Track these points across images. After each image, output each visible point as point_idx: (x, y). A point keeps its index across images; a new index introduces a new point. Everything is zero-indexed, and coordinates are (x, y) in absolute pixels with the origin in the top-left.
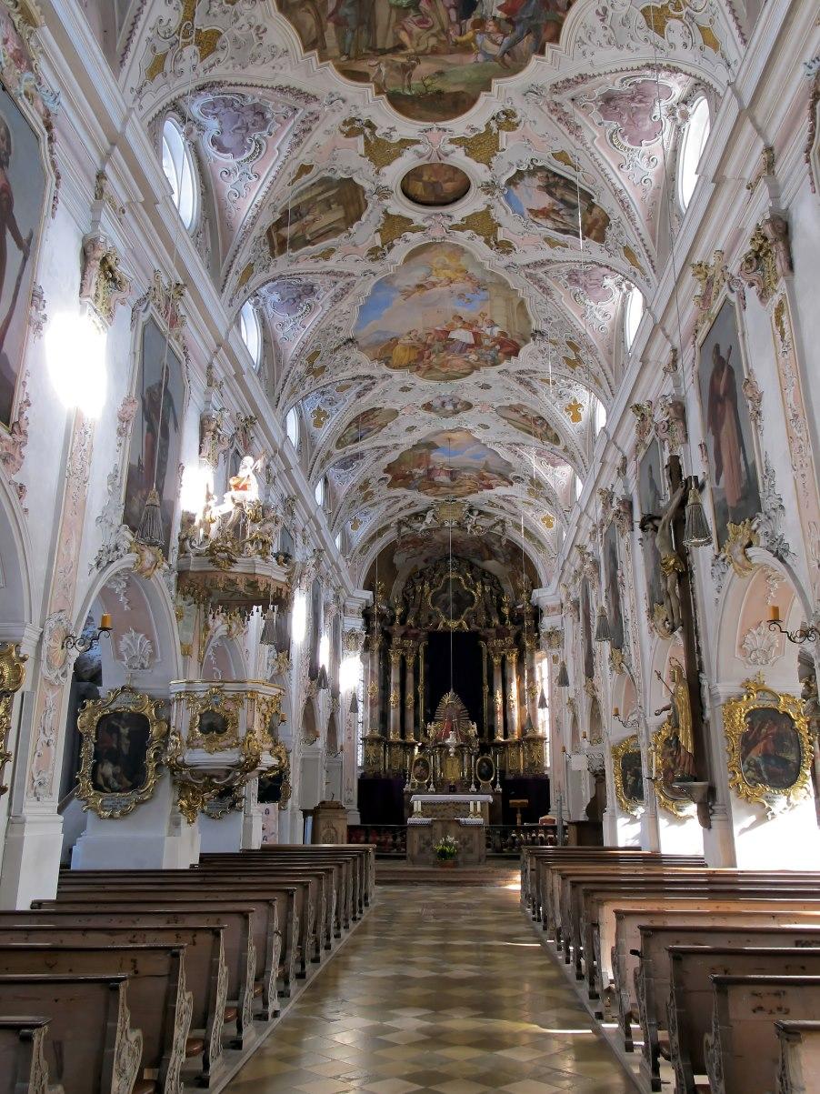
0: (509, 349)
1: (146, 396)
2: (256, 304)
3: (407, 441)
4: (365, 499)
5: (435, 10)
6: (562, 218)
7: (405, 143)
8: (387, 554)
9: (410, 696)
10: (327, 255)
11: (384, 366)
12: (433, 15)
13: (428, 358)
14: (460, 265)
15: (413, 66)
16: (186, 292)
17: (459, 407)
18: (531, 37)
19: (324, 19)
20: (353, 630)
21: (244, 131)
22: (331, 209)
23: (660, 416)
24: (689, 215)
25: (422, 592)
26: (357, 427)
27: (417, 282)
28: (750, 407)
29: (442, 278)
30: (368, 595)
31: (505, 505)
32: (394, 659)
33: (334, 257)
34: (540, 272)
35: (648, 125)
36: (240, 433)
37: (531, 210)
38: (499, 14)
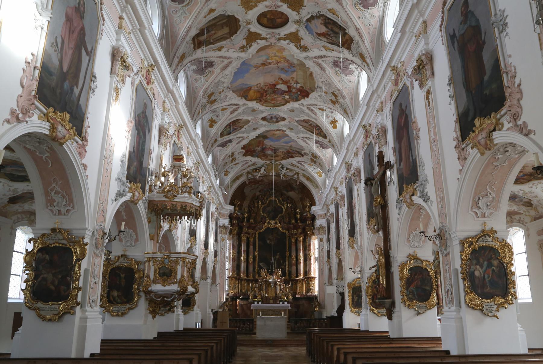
0: (304, 94)
1: (137, 119)
2: (184, 70)
3: (254, 135)
4: (232, 161)
8: (242, 187)
9: (251, 257)
10: (220, 49)
11: (244, 99)
13: (265, 97)
16: (155, 68)
17: (279, 119)
20: (224, 225)
23: (374, 132)
24: (389, 46)
25: (258, 206)
26: (230, 128)
27: (262, 62)
28: (415, 134)
29: (274, 61)
30: (232, 208)
31: (299, 165)
32: (244, 238)
33: (224, 50)
34: (320, 61)
36: (176, 133)
37: (317, 33)
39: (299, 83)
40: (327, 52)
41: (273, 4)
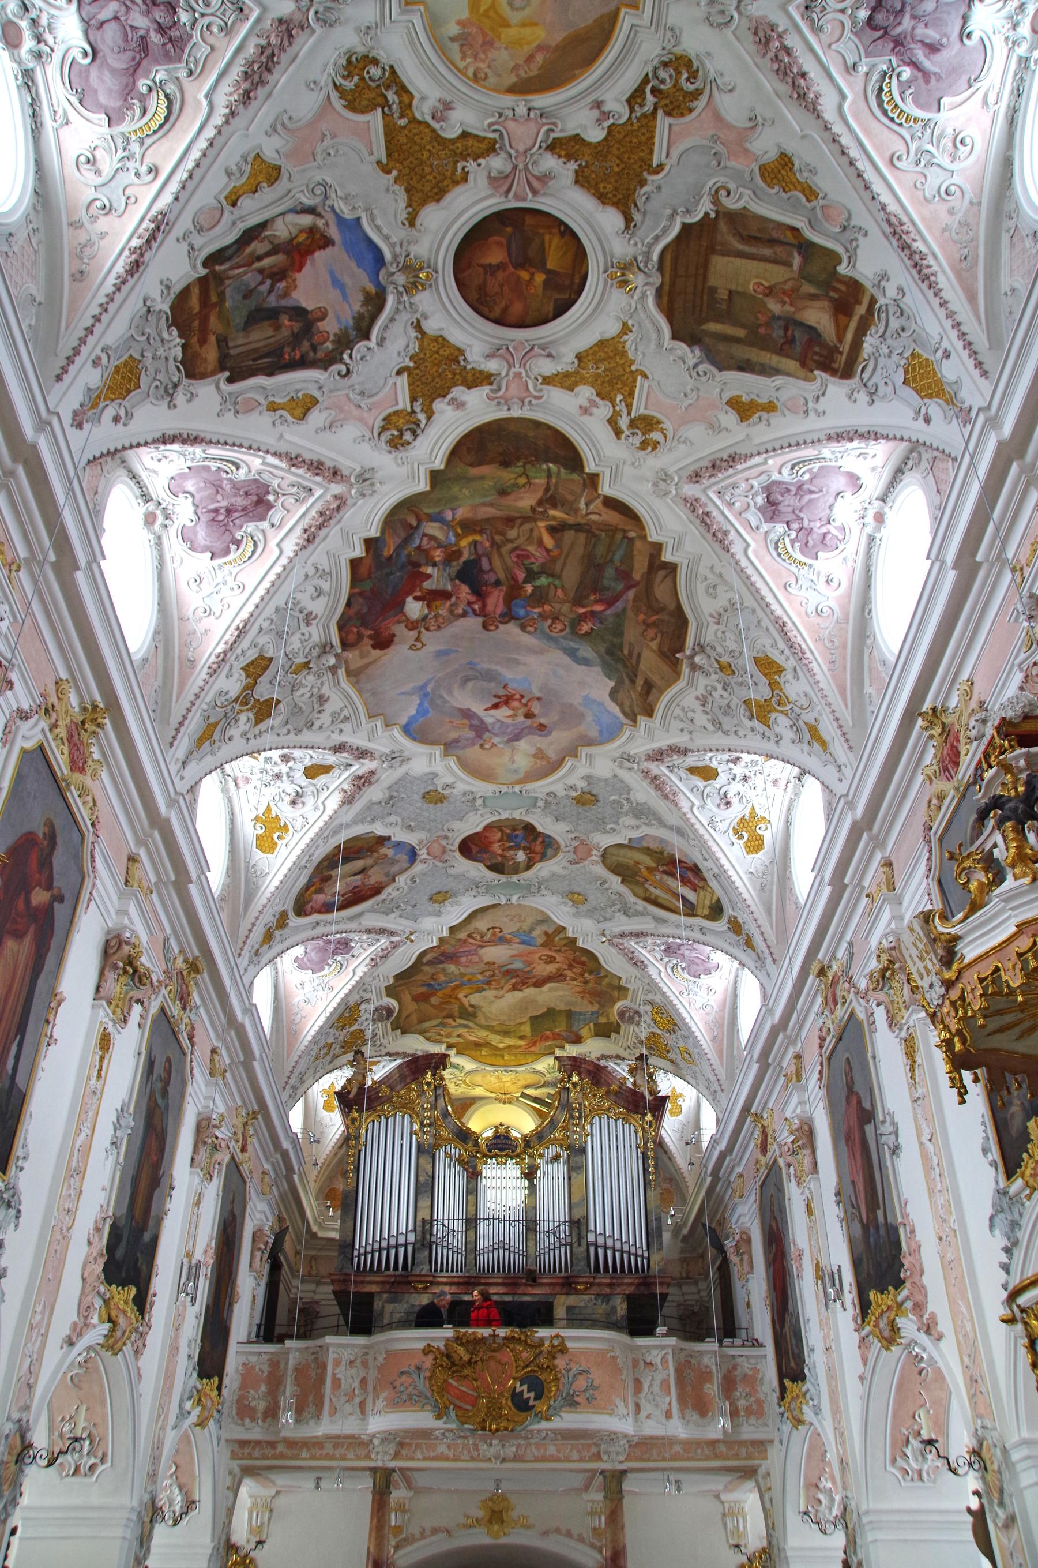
5: (506, 568)
6: (261, 271)
7: (566, 381)
12: (510, 564)
15: (540, 503)
16: (927, 706)
18: (386, 553)
21: (806, 487)
37: (327, 242)
38: (429, 570)
41: (517, 369)
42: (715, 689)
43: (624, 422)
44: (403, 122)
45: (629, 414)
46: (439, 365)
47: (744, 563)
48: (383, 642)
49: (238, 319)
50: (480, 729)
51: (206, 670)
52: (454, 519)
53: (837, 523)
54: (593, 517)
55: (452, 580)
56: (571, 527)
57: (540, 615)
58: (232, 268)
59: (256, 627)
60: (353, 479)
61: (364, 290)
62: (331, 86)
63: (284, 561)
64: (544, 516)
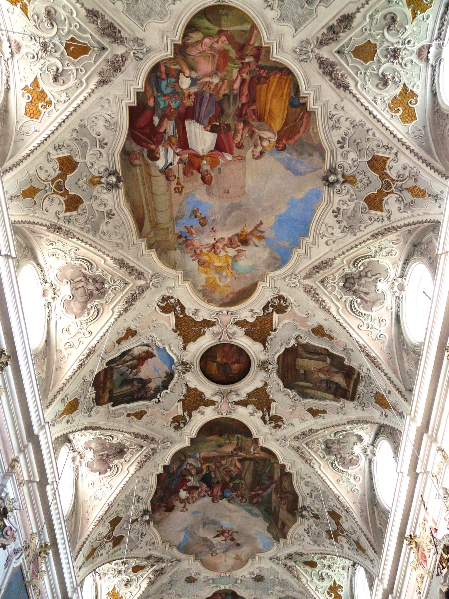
6: (127, 366)
7: (244, 403)
12: (223, 475)
13: (243, 81)
14: (206, 273)
15: (235, 450)
19: (278, 482)
22: (305, 371)
35: (93, 445)
37: (152, 356)
38: (190, 478)
39: (162, 171)
40: (126, 326)
42: (312, 526)
43: (267, 418)
44: (182, 316)
45: (269, 415)
46: (194, 398)
47: (319, 472)
48: (170, 509)
49: (117, 383)
50: (211, 546)
51: (93, 524)
52: (200, 457)
53: (356, 455)
54: (256, 455)
55: (199, 482)
56: (248, 459)
57: (236, 495)
58: (117, 365)
59: (117, 503)
60: (159, 442)
61: (166, 372)
62: (156, 305)
63: (130, 475)
64: (237, 455)
